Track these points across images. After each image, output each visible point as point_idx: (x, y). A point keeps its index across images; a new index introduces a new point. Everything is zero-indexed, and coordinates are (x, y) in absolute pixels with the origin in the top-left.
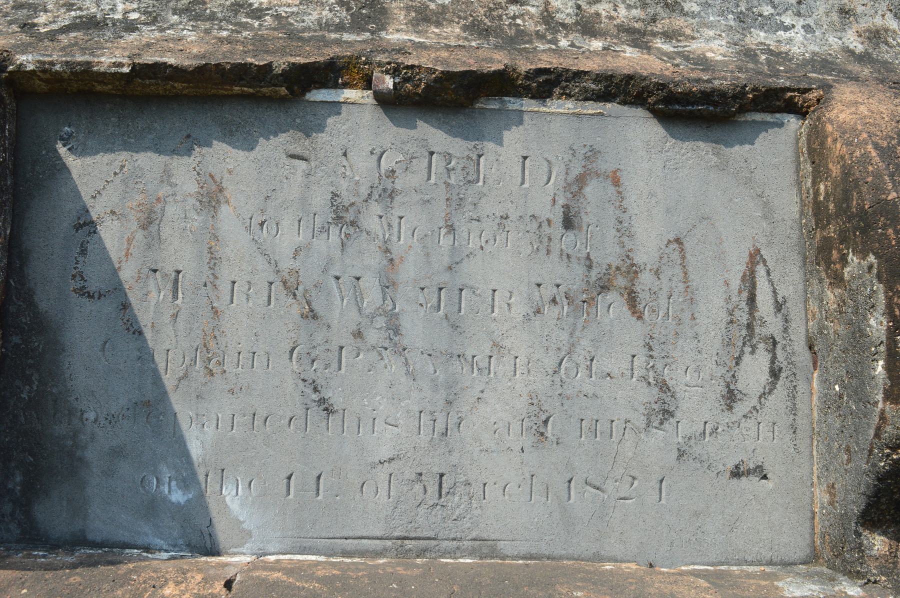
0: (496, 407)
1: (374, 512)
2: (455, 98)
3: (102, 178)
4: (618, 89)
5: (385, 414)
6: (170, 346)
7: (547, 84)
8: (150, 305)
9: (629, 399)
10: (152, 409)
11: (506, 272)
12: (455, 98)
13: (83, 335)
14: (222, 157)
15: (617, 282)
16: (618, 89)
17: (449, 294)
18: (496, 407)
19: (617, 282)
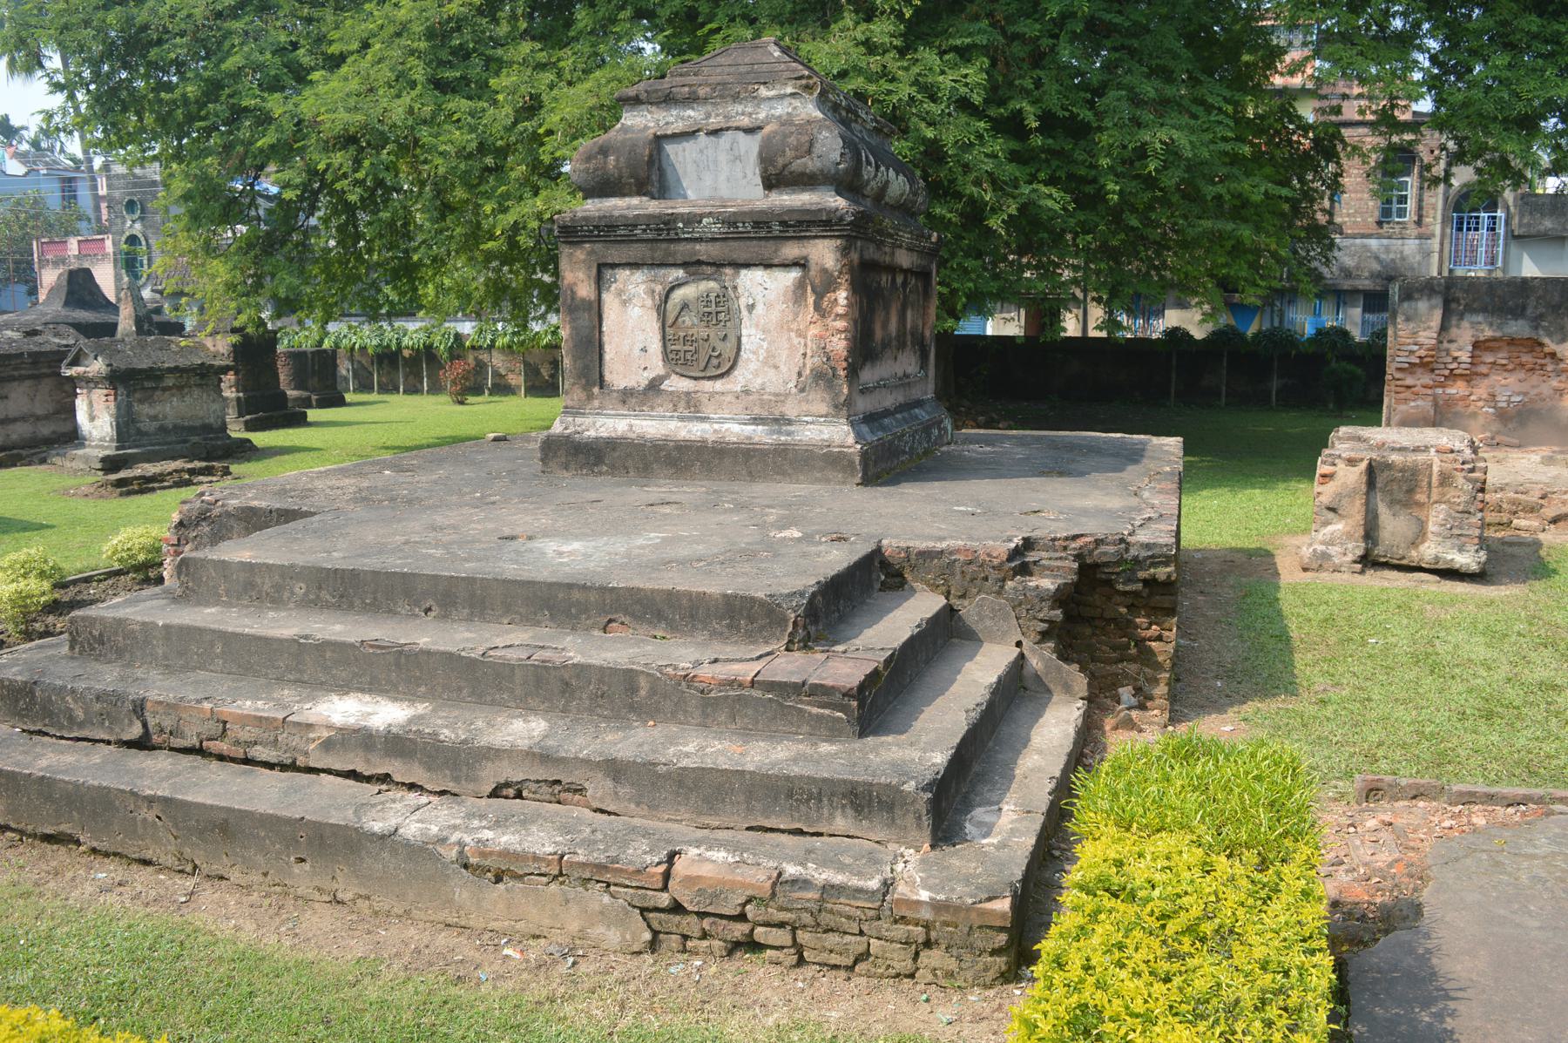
0: (722, 177)
1: (707, 194)
2: (715, 133)
3: (670, 149)
4: (737, 129)
5: (708, 180)
6: (680, 172)
7: (728, 129)
8: (677, 166)
9: (740, 175)
10: (679, 180)
11: (723, 158)
12: (715, 133)
13: (669, 171)
14: (685, 144)
15: (738, 158)
16: (737, 129)
17: (716, 162)
18: (722, 177)
19: (738, 158)
